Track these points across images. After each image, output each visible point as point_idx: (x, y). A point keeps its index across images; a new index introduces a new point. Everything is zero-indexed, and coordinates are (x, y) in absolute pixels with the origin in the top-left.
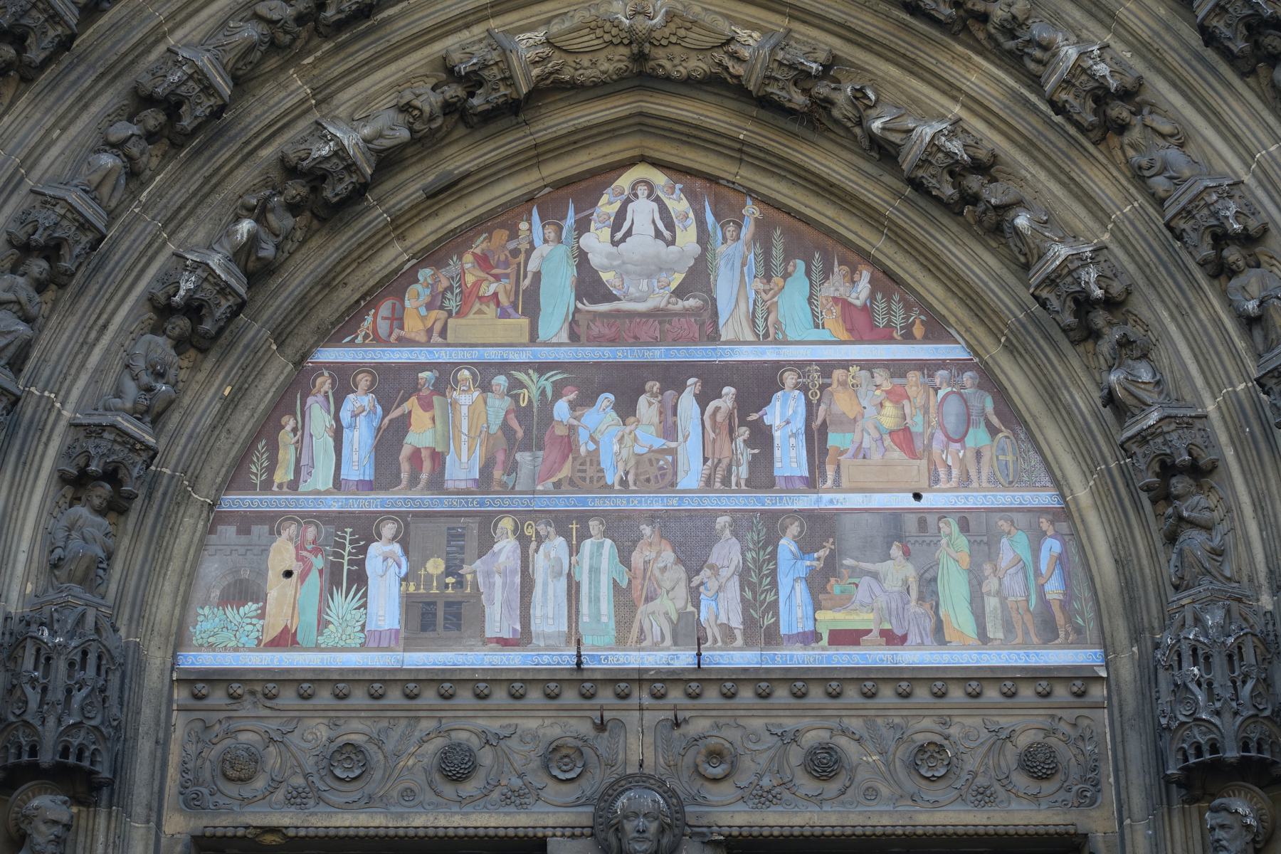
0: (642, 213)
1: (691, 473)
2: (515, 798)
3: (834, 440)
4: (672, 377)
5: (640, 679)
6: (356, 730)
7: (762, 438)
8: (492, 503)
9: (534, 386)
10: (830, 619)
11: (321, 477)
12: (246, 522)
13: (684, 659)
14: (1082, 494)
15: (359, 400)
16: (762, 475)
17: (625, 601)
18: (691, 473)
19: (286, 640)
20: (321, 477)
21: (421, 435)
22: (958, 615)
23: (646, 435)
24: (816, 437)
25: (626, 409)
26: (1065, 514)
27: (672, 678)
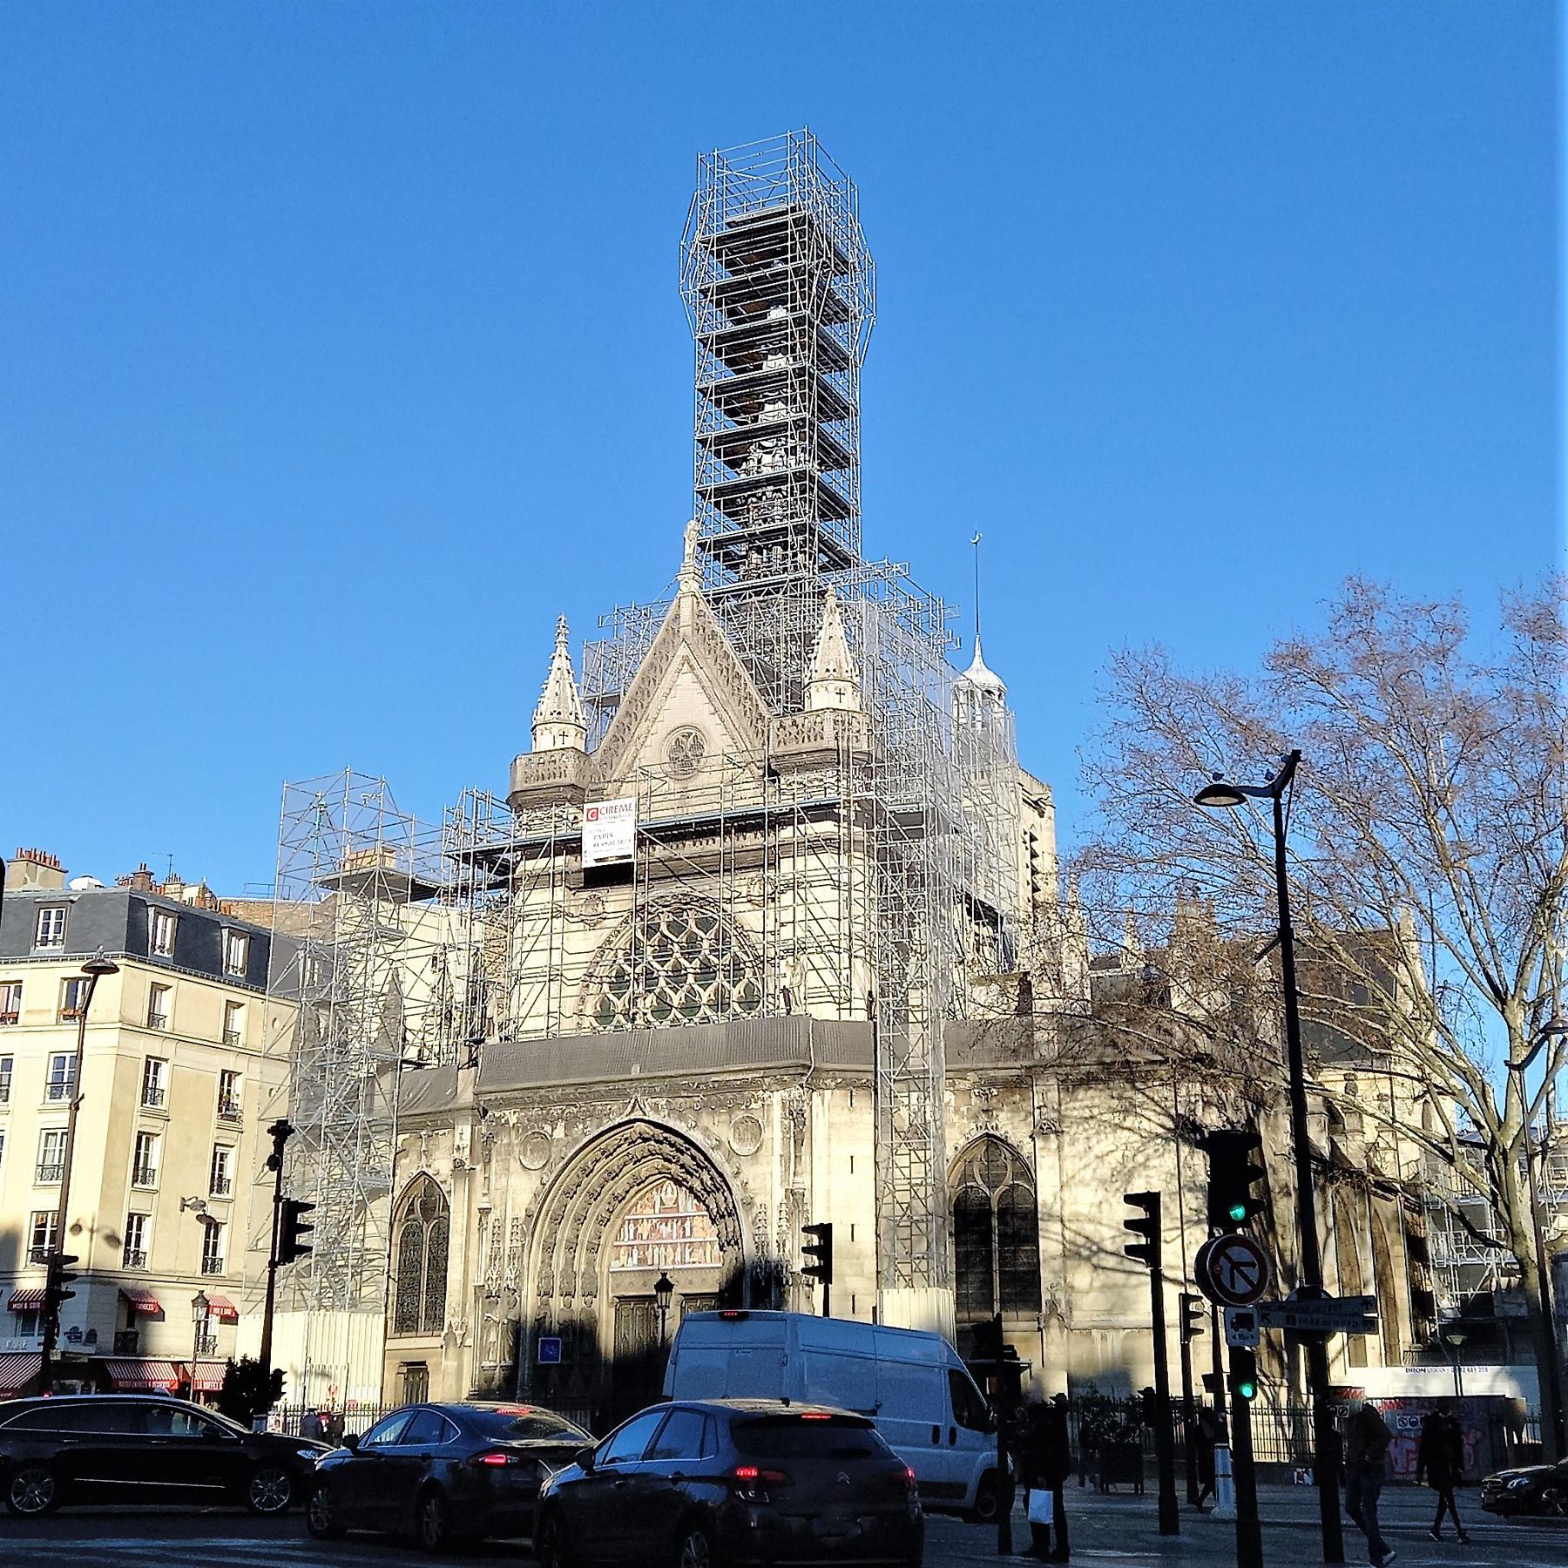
0: (669, 1189)
1: (675, 1237)
3: (694, 1229)
7: (684, 1229)
8: (649, 1242)
9: (655, 1221)
10: (692, 1260)
11: (626, 1239)
12: (617, 1246)
15: (632, 1225)
16: (684, 1236)
18: (675, 1237)
19: (623, 1266)
20: (626, 1239)
21: (639, 1231)
22: (708, 1259)
23: (670, 1230)
24: (691, 1228)
25: (666, 1225)
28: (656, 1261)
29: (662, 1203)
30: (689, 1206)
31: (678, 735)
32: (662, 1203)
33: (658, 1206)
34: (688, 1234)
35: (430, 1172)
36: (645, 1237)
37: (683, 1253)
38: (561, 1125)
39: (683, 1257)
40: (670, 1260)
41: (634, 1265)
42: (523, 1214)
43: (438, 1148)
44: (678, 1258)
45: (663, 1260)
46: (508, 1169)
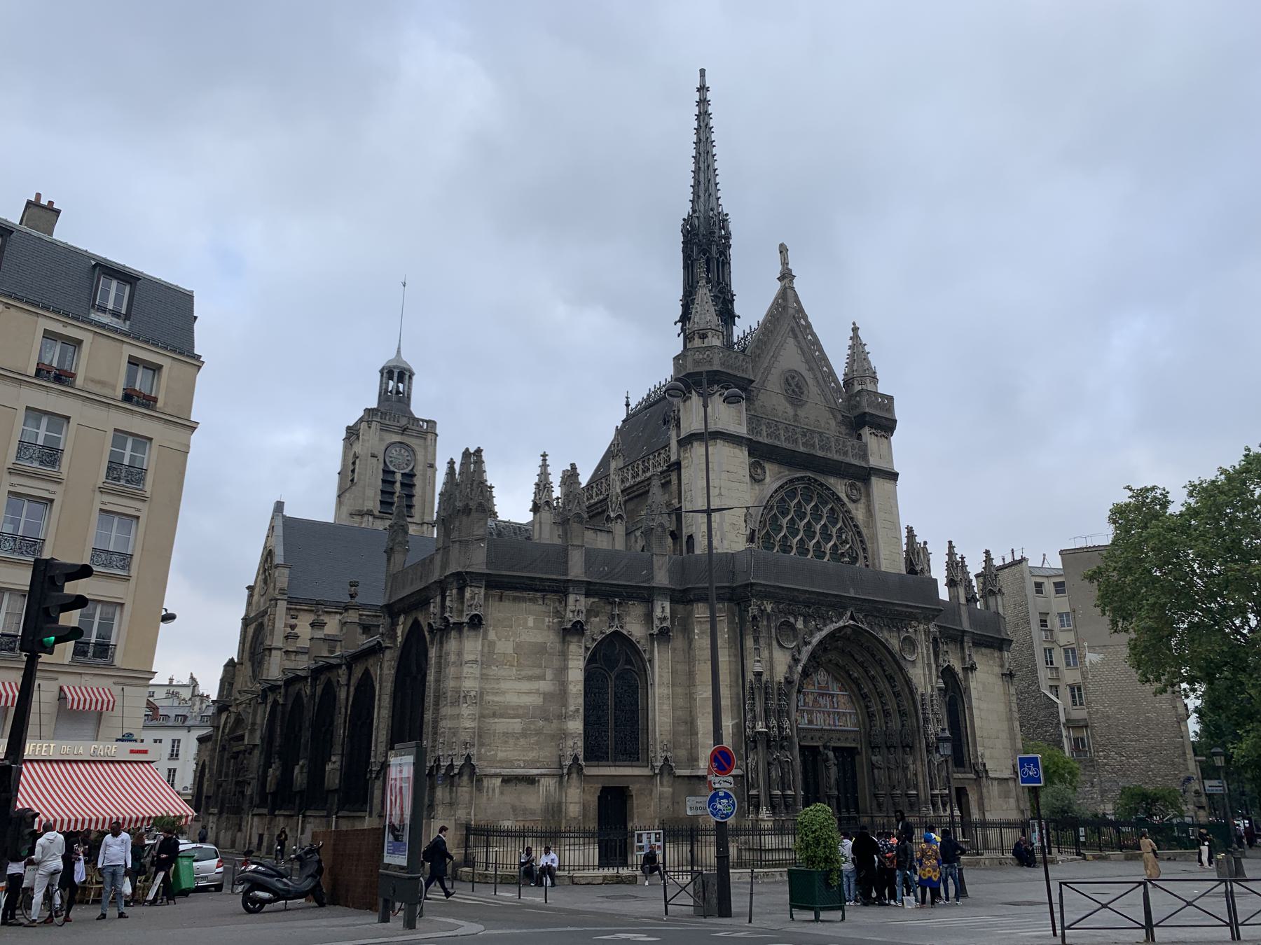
2: (817, 742)
4: (826, 694)
5: (827, 730)
6: (804, 734)
13: (829, 728)
14: (859, 711)
17: (824, 721)
21: (807, 701)
26: (856, 714)
27: (829, 730)
28: (819, 723)
29: (819, 683)
30: (835, 689)
31: (788, 374)
32: (819, 683)
33: (816, 684)
34: (836, 706)
35: (625, 633)
36: (810, 705)
37: (834, 719)
38: (800, 619)
39: (834, 722)
40: (827, 722)
41: (805, 724)
42: (783, 681)
43: (628, 614)
44: (832, 722)
45: (822, 721)
46: (770, 645)
